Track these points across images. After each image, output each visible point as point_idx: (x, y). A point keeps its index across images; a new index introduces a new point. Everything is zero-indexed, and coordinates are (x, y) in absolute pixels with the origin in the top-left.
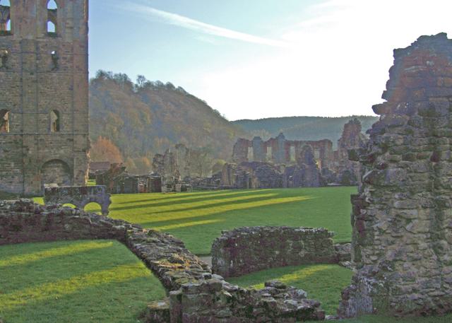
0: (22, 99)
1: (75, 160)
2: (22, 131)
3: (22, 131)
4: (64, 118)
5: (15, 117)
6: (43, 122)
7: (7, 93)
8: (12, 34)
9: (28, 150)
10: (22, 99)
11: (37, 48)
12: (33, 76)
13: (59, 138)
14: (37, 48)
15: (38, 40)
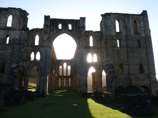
0: (128, 59)
1: (152, 86)
2: (129, 73)
3: (129, 73)
4: (145, 67)
5: (125, 67)
6: (137, 69)
7: (122, 57)
8: (122, 33)
9: (132, 81)
10: (128, 59)
11: (132, 38)
12: (132, 50)
13: (143, 76)
14: (132, 38)
15: (132, 35)
